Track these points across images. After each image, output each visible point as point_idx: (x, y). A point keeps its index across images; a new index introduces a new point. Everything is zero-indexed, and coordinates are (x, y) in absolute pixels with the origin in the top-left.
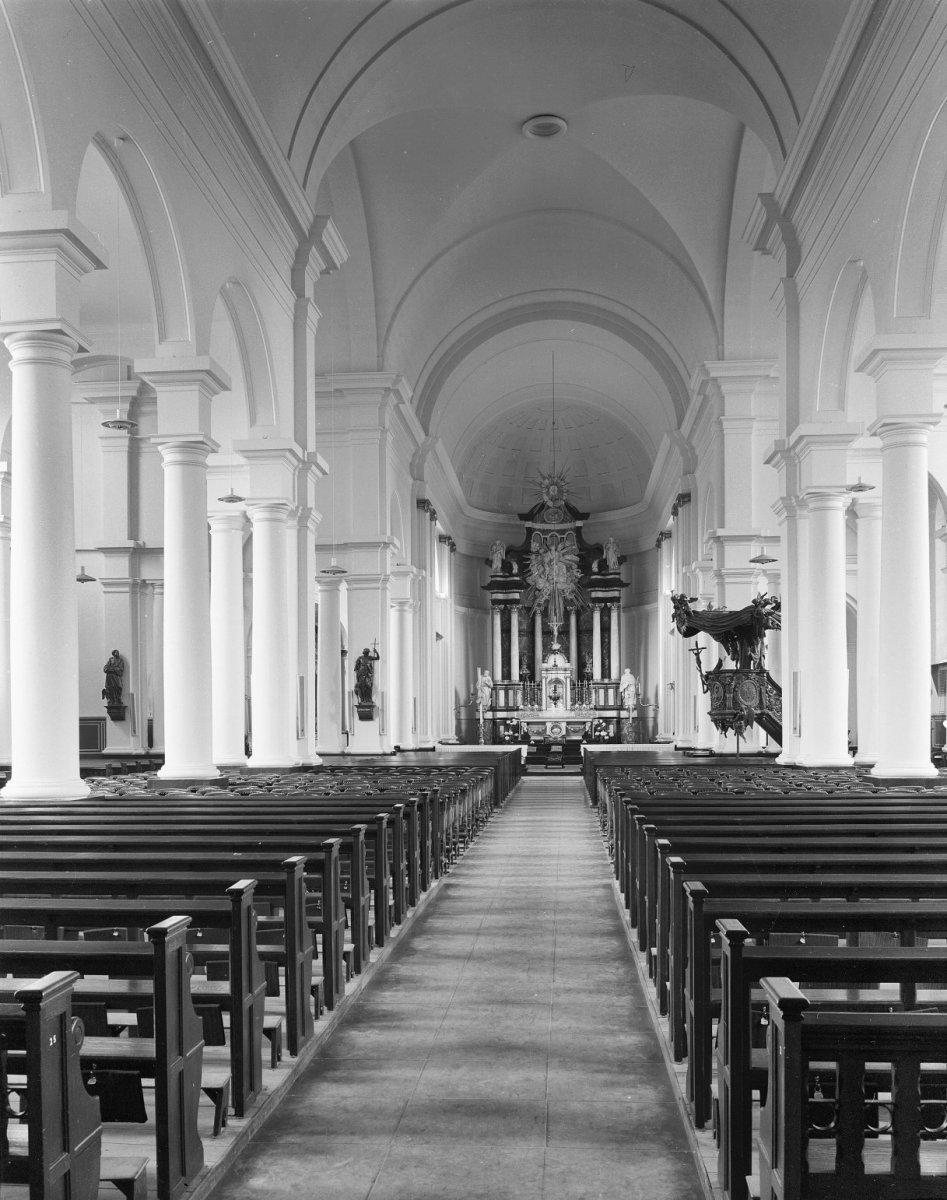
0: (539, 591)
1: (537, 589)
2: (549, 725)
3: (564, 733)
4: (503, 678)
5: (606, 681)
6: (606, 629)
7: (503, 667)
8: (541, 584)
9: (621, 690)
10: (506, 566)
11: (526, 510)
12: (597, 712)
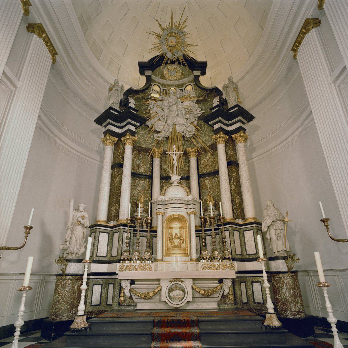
0: (158, 132)
1: (155, 131)
2: (165, 286)
3: (189, 298)
4: (109, 219)
5: (240, 221)
6: (233, 163)
7: (110, 205)
8: (159, 126)
9: (264, 228)
10: (124, 103)
11: (147, 58)
12: (235, 263)
